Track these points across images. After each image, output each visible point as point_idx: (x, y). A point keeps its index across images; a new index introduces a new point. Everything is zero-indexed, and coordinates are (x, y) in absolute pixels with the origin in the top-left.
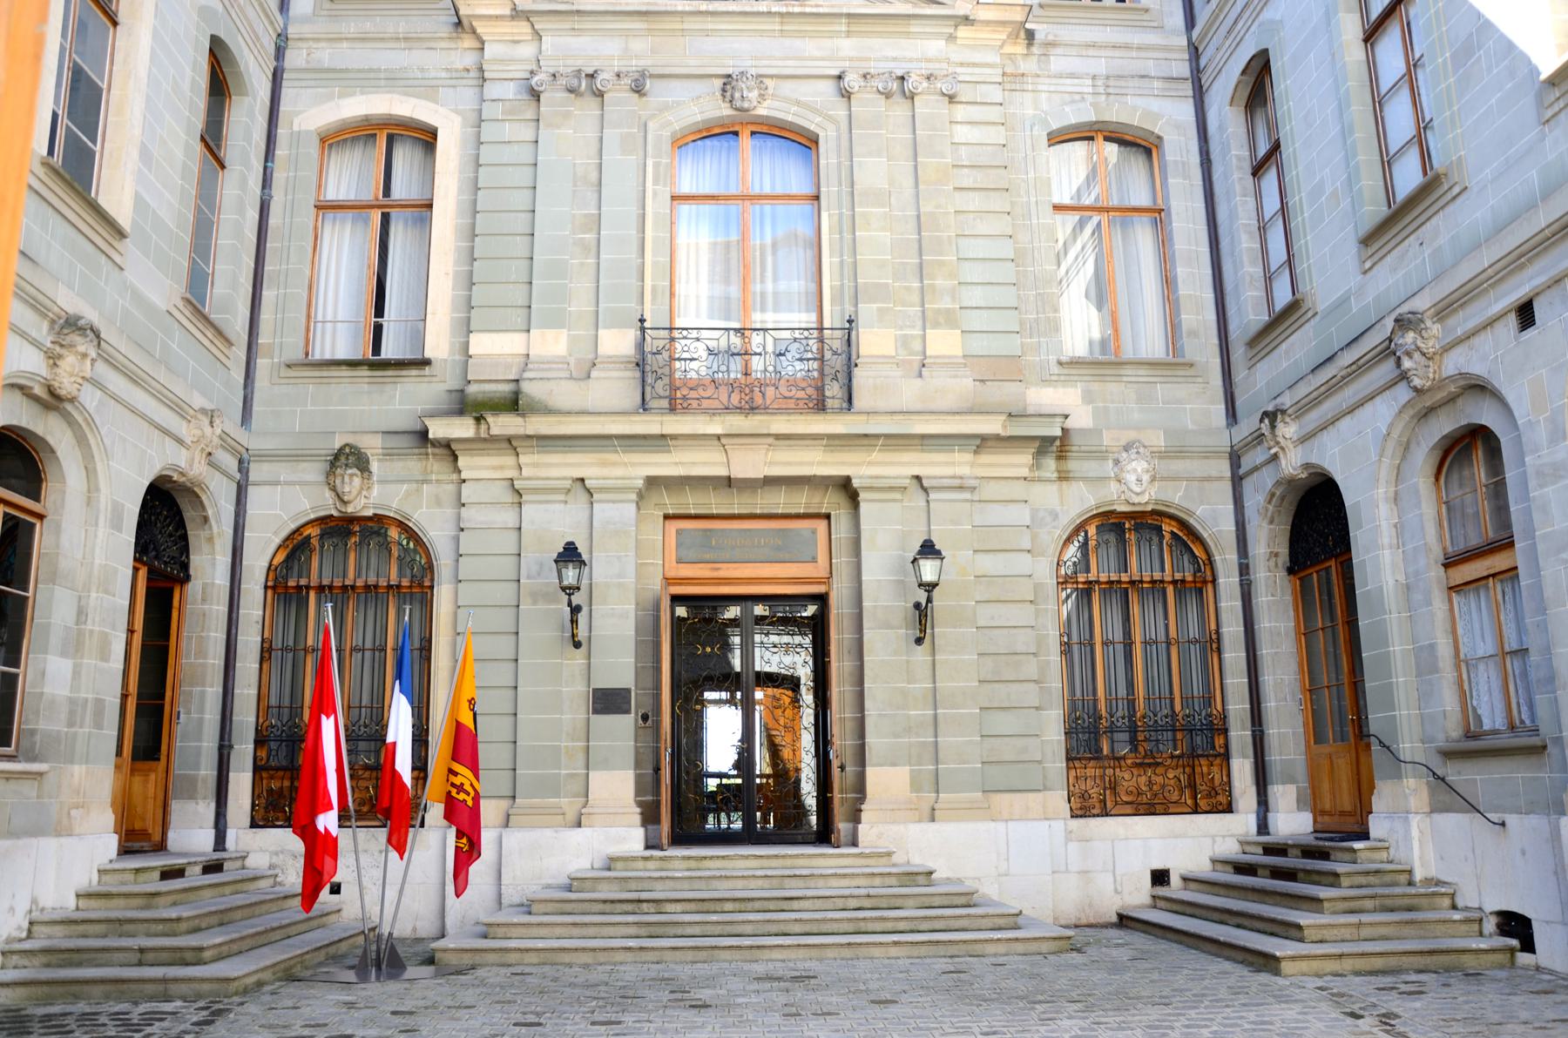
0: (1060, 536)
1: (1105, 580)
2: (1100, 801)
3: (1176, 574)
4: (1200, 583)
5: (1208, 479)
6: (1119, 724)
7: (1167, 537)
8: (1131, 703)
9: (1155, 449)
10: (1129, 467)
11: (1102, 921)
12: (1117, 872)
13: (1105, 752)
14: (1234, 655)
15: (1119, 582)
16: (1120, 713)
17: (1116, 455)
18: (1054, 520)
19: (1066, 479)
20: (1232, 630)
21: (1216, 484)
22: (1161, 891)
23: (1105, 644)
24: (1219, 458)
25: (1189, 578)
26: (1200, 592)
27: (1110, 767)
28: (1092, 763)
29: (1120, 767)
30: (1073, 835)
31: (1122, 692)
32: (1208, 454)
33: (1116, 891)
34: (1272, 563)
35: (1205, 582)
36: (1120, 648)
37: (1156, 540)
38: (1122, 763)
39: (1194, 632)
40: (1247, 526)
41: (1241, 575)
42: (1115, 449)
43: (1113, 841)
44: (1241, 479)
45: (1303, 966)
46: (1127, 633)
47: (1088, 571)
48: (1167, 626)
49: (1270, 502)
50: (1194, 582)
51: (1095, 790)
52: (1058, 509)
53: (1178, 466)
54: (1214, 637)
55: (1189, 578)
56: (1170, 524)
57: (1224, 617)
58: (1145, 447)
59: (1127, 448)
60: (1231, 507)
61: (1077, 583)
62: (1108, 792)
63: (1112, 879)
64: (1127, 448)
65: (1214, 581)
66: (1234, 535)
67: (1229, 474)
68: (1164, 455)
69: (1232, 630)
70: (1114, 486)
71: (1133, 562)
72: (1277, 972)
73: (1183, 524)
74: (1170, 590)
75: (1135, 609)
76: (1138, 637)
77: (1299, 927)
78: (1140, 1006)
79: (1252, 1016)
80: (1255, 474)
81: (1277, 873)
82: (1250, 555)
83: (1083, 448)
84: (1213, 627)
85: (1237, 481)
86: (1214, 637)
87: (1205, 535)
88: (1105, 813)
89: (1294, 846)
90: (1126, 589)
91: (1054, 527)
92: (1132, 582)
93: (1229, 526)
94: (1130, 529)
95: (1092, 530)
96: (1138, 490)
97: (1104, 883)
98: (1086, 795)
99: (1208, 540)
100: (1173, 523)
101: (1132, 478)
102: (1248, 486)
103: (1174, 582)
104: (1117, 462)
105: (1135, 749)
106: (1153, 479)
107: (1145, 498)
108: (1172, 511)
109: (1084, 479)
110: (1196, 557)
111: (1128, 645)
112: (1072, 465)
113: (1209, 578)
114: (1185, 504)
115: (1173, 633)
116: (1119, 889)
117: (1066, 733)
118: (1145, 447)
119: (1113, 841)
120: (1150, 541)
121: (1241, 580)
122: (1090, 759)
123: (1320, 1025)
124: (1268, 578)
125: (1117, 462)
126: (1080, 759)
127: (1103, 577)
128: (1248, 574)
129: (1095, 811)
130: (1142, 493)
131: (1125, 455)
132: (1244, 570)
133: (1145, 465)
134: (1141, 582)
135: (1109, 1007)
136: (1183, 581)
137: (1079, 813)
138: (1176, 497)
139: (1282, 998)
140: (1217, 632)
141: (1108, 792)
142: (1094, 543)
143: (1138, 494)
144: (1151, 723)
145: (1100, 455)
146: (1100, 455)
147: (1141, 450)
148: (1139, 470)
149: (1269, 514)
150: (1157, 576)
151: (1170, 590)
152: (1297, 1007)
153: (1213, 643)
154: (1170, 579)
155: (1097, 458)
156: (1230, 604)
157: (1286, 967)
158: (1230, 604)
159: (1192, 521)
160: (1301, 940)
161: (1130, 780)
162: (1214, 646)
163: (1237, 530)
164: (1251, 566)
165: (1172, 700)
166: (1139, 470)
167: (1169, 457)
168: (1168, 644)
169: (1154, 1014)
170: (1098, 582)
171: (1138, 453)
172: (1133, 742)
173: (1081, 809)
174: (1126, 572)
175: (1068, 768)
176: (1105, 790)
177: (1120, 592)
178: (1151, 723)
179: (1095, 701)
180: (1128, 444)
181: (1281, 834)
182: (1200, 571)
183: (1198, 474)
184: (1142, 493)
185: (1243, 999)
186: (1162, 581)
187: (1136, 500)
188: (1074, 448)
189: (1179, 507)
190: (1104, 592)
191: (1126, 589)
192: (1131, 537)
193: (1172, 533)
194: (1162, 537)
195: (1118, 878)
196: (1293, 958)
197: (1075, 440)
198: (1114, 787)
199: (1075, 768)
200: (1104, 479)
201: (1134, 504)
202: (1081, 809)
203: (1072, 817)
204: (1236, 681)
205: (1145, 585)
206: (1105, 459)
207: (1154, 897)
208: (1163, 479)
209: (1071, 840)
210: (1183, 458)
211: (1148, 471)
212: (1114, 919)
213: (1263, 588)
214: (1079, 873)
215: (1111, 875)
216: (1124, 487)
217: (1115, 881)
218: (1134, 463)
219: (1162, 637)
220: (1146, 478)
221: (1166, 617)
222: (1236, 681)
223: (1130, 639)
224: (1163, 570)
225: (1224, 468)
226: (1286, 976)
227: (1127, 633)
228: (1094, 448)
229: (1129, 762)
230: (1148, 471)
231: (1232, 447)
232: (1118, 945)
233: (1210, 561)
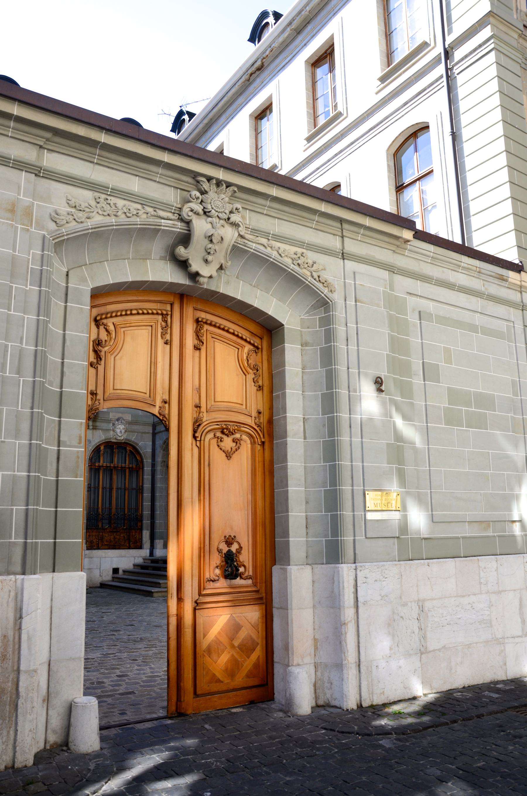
0: (91, 449)
1: (105, 465)
2: (97, 544)
3: (130, 465)
4: (139, 468)
5: (145, 433)
6: (106, 517)
7: (128, 452)
8: (110, 509)
9: (127, 421)
10: (118, 427)
11: (94, 586)
12: (101, 569)
13: (100, 527)
14: (147, 495)
15: (110, 467)
16: (106, 513)
17: (114, 422)
18: (90, 443)
19: (95, 429)
20: (147, 485)
21: (147, 435)
22: (116, 576)
23: (103, 488)
24: (149, 426)
25: (134, 467)
26: (137, 472)
27: (101, 532)
28: (95, 531)
29: (105, 532)
30: (87, 556)
31: (108, 506)
32: (145, 424)
33: (100, 575)
34: (163, 464)
35: (140, 468)
36: (108, 490)
37: (124, 451)
38: (106, 531)
39: (134, 486)
40: (156, 451)
41: (152, 467)
42: (113, 420)
43: (100, 558)
44: (156, 434)
45: (160, 594)
46: (111, 484)
47: (99, 462)
48: (125, 483)
49: (164, 444)
50: (136, 468)
51: (96, 540)
52: (91, 439)
53: (135, 427)
54: (141, 488)
55: (134, 467)
56: (130, 447)
57: (145, 481)
58: (124, 420)
59: (118, 420)
60: (151, 443)
61: (95, 466)
62: (100, 541)
63: (99, 572)
64: (118, 420)
65: (143, 468)
66: (151, 453)
67: (151, 432)
68: (130, 423)
69: (147, 485)
70: (112, 433)
71: (116, 460)
72: (152, 596)
73: (134, 448)
74: (127, 470)
75: (115, 477)
76: (115, 487)
77: (160, 584)
79: (144, 606)
80: (160, 434)
81: (155, 569)
82: (156, 460)
83: (102, 418)
84: (141, 484)
85: (154, 434)
86: (141, 488)
87: (141, 452)
88: (98, 548)
89: (161, 560)
90: (112, 469)
91: (89, 446)
92: (114, 467)
93: (149, 450)
94: (115, 448)
95: (102, 448)
96: (120, 435)
97: (97, 573)
98: (92, 542)
99: (142, 454)
100: (131, 447)
101: (118, 431)
102: (158, 437)
103: (129, 468)
104: (114, 424)
105: (110, 526)
106: (126, 431)
107: (122, 438)
108: (131, 443)
109: (102, 429)
110: (137, 460)
111: (111, 489)
112: (98, 424)
113: (141, 467)
114: (136, 441)
115: (127, 486)
116: (101, 575)
117: (87, 520)
118: (124, 420)
119: (100, 558)
120: (122, 453)
121: (152, 469)
122: (95, 529)
123: (162, 607)
124: (161, 469)
125: (114, 424)
126: (91, 529)
127: (105, 465)
128: (154, 467)
129: (95, 548)
130: (122, 436)
131: (117, 422)
132: (153, 465)
133: (123, 427)
134: (118, 467)
136: (132, 468)
137: (89, 548)
138: (133, 438)
139: (152, 602)
140: (142, 486)
141: (100, 541)
142: (102, 452)
143: (120, 436)
144: (116, 517)
145: (108, 421)
146: (108, 421)
147: (123, 421)
148: (121, 428)
149: (164, 448)
150: (123, 465)
151: (127, 470)
152: (157, 604)
153: (140, 490)
154: (127, 466)
155: (107, 422)
156: (147, 477)
157: (155, 595)
158: (147, 477)
159: (137, 447)
160: (160, 588)
161: (107, 537)
162: (141, 491)
163: (152, 452)
164: (156, 464)
165: (124, 509)
166: (121, 428)
167: (133, 424)
168: (125, 489)
169: (117, 606)
170: (103, 466)
171: (121, 422)
172: (110, 523)
173: (90, 546)
174: (113, 463)
175: (87, 532)
176: (99, 540)
177: (110, 470)
178: (116, 517)
179: (98, 509)
180: (118, 418)
181: (157, 556)
182: (138, 464)
183: (141, 431)
184: (122, 436)
185: (142, 603)
186: (125, 467)
187: (119, 438)
188: (99, 418)
189: (133, 442)
190: (104, 470)
191: (112, 469)
192: (116, 451)
193: (130, 450)
194: (126, 452)
195: (101, 571)
196: (157, 592)
197: (100, 415)
198: (102, 539)
199: (89, 532)
200: (109, 430)
201: (118, 440)
202: (90, 546)
203: (87, 549)
204: (147, 504)
205: (119, 468)
206: (110, 423)
207: (113, 578)
208: (129, 432)
209: (86, 558)
210: (137, 425)
211: (124, 429)
212: (99, 585)
213: (159, 473)
214: (88, 569)
215: (99, 570)
216: (115, 434)
217: (100, 572)
218: (120, 426)
219: (123, 487)
220: (123, 431)
221: (125, 480)
222: (147, 504)
223: (112, 487)
224: (125, 463)
225: (150, 429)
226: (154, 597)
227: (111, 484)
228: (106, 419)
229: (108, 530)
230: (124, 429)
231: (154, 422)
232: (102, 592)
233: (142, 461)
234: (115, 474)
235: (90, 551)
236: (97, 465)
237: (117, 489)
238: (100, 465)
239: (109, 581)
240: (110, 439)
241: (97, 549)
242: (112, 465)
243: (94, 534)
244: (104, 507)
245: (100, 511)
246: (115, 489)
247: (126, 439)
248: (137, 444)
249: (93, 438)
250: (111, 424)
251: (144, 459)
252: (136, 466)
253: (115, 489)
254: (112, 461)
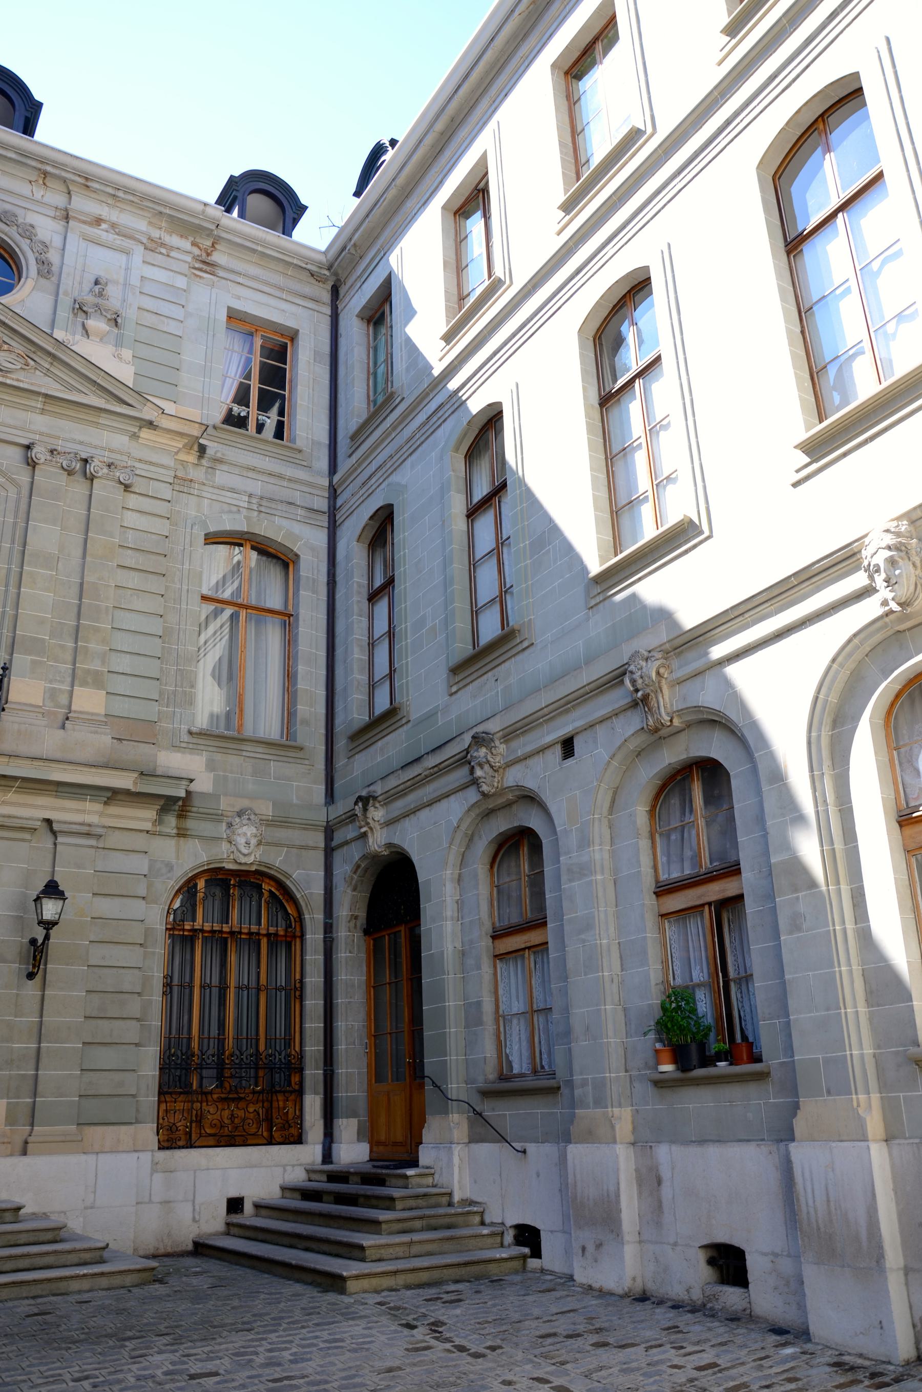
0: (173, 886)
2: (186, 1133)
3: (270, 928)
6: (209, 1061)
7: (266, 894)
8: (221, 1042)
9: (264, 817)
10: (240, 831)
12: (197, 1202)
13: (194, 1088)
14: (314, 1003)
15: (221, 932)
16: (211, 1052)
18: (169, 871)
20: (314, 979)
22: (236, 1219)
23: (202, 987)
24: (315, 830)
25: (281, 933)
26: (289, 946)
27: (198, 1101)
28: (182, 1098)
29: (207, 1101)
31: (214, 1032)
32: (308, 826)
33: (194, 1220)
34: (352, 924)
35: (294, 937)
36: (215, 991)
37: (256, 897)
38: (209, 1097)
41: (325, 933)
42: (229, 814)
43: (195, 1171)
44: (333, 850)
45: (365, 1283)
47: (194, 920)
48: (258, 974)
49: (355, 873)
50: (285, 936)
52: (174, 861)
53: (281, 834)
54: (298, 985)
55: (281, 933)
56: (268, 884)
57: (308, 968)
58: (256, 815)
60: (322, 873)
61: (184, 930)
62: (194, 1125)
63: (191, 1209)
64: (240, 814)
65: (302, 936)
67: (322, 845)
68: (271, 823)
69: (314, 979)
70: (225, 846)
71: (235, 914)
72: (342, 1291)
75: (232, 958)
76: (233, 983)
77: (362, 1248)
78: (225, 1333)
79: (325, 1335)
80: (345, 847)
81: (341, 1199)
83: (201, 810)
84: (298, 977)
85: (329, 851)
86: (298, 985)
87: (298, 896)
88: (190, 1145)
89: (355, 1174)
90: (226, 939)
91: (168, 878)
92: (232, 933)
93: (318, 889)
94: (234, 886)
95: (201, 884)
96: (245, 851)
97: (184, 1212)
98: (174, 1128)
99: (301, 901)
100: (272, 883)
101: (241, 841)
102: (338, 856)
103: (268, 935)
104: (230, 825)
105: (220, 1085)
106: (259, 843)
107: (251, 859)
108: (272, 872)
109: (199, 837)
111: (223, 988)
112: (191, 824)
113: (298, 933)
116: (197, 1217)
117: (160, 1069)
118: (256, 815)
119: (195, 1171)
121: (325, 938)
122: (181, 1093)
123: (383, 1338)
124: (347, 937)
125: (230, 825)
126: (171, 1093)
127: (207, 927)
128: (331, 932)
129: (181, 1143)
131: (237, 820)
132: (328, 928)
133: (254, 831)
134: (240, 933)
135: (195, 1337)
136: (276, 935)
137: (165, 1144)
138: (277, 860)
139: (349, 1315)
140: (301, 981)
141: (194, 1125)
142: (202, 895)
143: (245, 855)
144: (237, 1061)
145: (217, 817)
146: (217, 817)
147: (252, 817)
148: (249, 834)
149: (354, 882)
150: (254, 928)
152: (363, 1323)
153: (296, 991)
154: (264, 932)
156: (314, 958)
157: (351, 1286)
158: (314, 958)
159: (288, 883)
160: (363, 1260)
161: (213, 1113)
162: (298, 993)
163: (325, 894)
164: (334, 926)
165: (257, 1040)
166: (249, 834)
168: (258, 989)
169: (238, 1341)
170: (202, 931)
171: (249, 819)
172: (220, 1078)
173: (168, 1141)
174: (227, 923)
175: (159, 1102)
179: (190, 1039)
181: (342, 1162)
182: (290, 926)
183: (297, 843)
185: (316, 1319)
186: (258, 934)
187: (243, 860)
188: (194, 809)
189: (279, 870)
191: (226, 939)
192: (235, 892)
193: (270, 891)
194: (261, 895)
195: (197, 1207)
196: (357, 1277)
197: (196, 802)
199: (166, 1102)
201: (240, 864)
202: (168, 1141)
203: (159, 1149)
204: (314, 1025)
205: (243, 936)
206: (220, 821)
207: (228, 1224)
208: (268, 844)
209: (157, 1172)
210: (287, 827)
211: (255, 836)
212: (190, 1247)
214: (161, 1203)
216: (233, 848)
217: (194, 1210)
219: (253, 984)
220: (254, 842)
221: (259, 966)
222: (314, 1025)
224: (259, 924)
225: (319, 839)
226: (350, 1295)
228: (211, 811)
229: (215, 1096)
231: (328, 822)
232: (196, 1274)
234: (234, 949)
235: (168, 1153)
236: (187, 927)
237: (239, 988)
238: (196, 927)
239: (217, 1234)
240: (221, 861)
241: (187, 1148)
242: (226, 928)
243: (179, 1106)
244: (206, 1035)
245: (195, 1044)
246: (232, 989)
247: (260, 863)
248: (289, 876)
249: (178, 858)
250: (224, 824)
251: (305, 912)
252: (286, 931)
253: (232, 989)
254: (225, 919)
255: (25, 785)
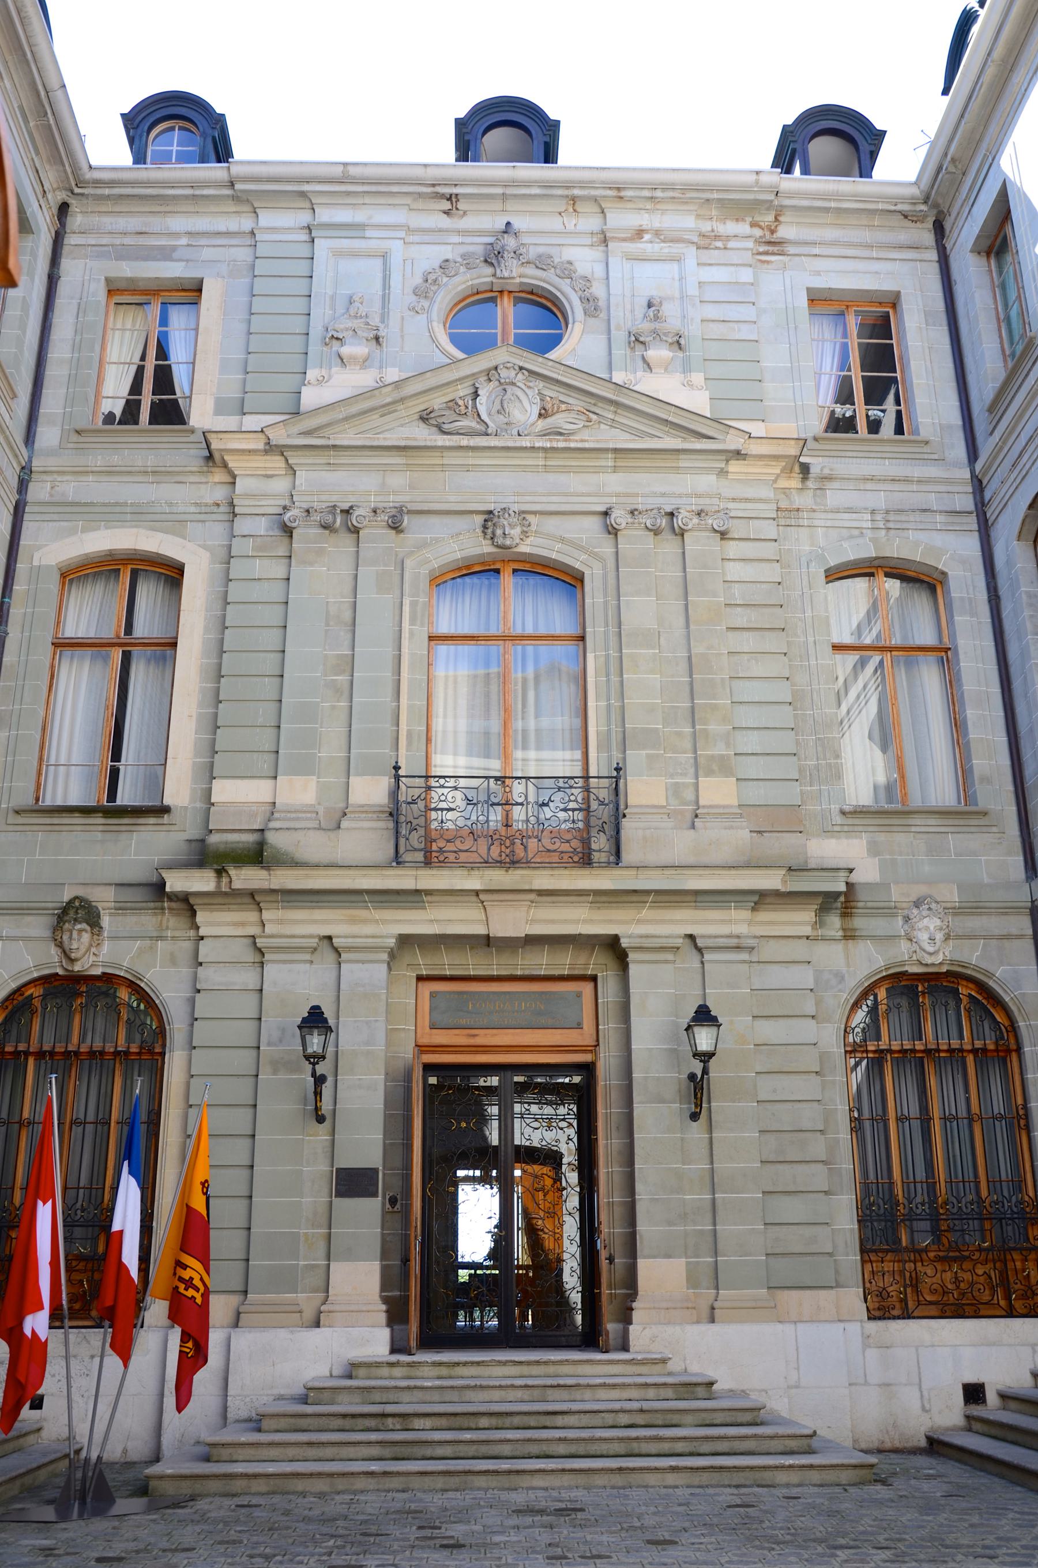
2: (901, 1301)
3: (976, 1042)
5: (1008, 937)
6: (919, 1211)
7: (965, 1000)
8: (931, 1187)
9: (949, 905)
10: (920, 925)
11: (909, 1445)
12: (924, 1387)
13: (904, 1244)
15: (914, 1051)
16: (919, 1199)
17: (906, 912)
19: (852, 937)
21: (1017, 943)
22: (976, 1410)
23: (900, 1119)
24: (1018, 914)
25: (991, 1047)
26: (1004, 1062)
27: (910, 1261)
28: (890, 1256)
29: (922, 1261)
30: (871, 1340)
31: (921, 1174)
32: (1007, 910)
33: (924, 1409)
35: (1008, 1051)
36: (916, 1124)
37: (952, 1004)
38: (924, 1256)
39: (999, 1107)
42: (904, 905)
43: (917, 1348)
47: (878, 1038)
48: (968, 1100)
50: (997, 1050)
52: (844, 970)
55: (991, 1047)
58: (937, 902)
59: (917, 904)
61: (867, 1052)
62: (909, 1290)
64: (917, 904)
65: (1019, 1050)
68: (958, 911)
70: (904, 946)
73: (982, 987)
74: (970, 1059)
75: (932, 1082)
76: (936, 1113)
78: (959, 1557)
83: (869, 904)
84: (1020, 1101)
86: (1021, 1112)
87: (1007, 999)
88: (906, 1315)
91: (840, 991)
92: (928, 1052)
94: (923, 993)
95: (882, 994)
96: (931, 949)
97: (910, 1399)
99: (1011, 1004)
101: (923, 937)
103: (974, 1051)
104: (907, 919)
105: (937, 1240)
106: (947, 938)
108: (969, 972)
111: (926, 1120)
112: (858, 922)
113: (1013, 1046)
114: (983, 965)
115: (975, 1109)
116: (927, 1407)
117: (859, 1221)
118: (937, 902)
122: (887, 1251)
125: (907, 919)
126: (875, 1251)
127: (896, 1046)
129: (896, 1312)
131: (915, 911)
133: (938, 922)
134: (938, 1050)
135: (922, 1556)
136: (984, 1050)
137: (877, 1314)
140: (1025, 1106)
141: (909, 1290)
142: (884, 1007)
143: (931, 954)
144: (955, 1210)
145: (889, 911)
146: (889, 911)
147: (933, 906)
148: (932, 928)
150: (955, 1043)
151: (970, 1059)
154: (969, 1047)
159: (991, 983)
161: (931, 1275)
162: (1022, 1122)
165: (977, 1183)
166: (932, 928)
168: (971, 1119)
170: (890, 1051)
171: (930, 909)
172: (936, 1233)
173: (879, 1309)
174: (921, 1039)
175: (863, 1262)
178: (955, 1210)
179: (891, 1184)
182: (1002, 1038)
183: (997, 932)
186: (961, 1050)
187: (929, 960)
188: (860, 904)
189: (977, 968)
190: (896, 1062)
192: (926, 1001)
193: (970, 996)
195: (925, 1393)
197: (862, 895)
198: (915, 1284)
199: (871, 1261)
201: (927, 965)
202: (879, 1309)
203: (869, 1318)
205: (942, 1055)
206: (894, 915)
207: (968, 1417)
208: (959, 937)
209: (870, 1347)
210: (980, 914)
211: (941, 929)
212: (923, 1443)
214: (879, 1385)
216: (915, 947)
217: (922, 1396)
218: (926, 920)
219: (963, 1112)
220: (939, 936)
221: (967, 1090)
223: (927, 1113)
229: (932, 1255)
230: (941, 929)
231: (1032, 902)
232: (929, 1477)
234: (932, 1071)
235: (881, 1324)
236: (871, 1048)
237: (944, 1119)
238: (881, 1047)
239: (954, 1429)
240: (902, 963)
241: (904, 1318)
242: (919, 1046)
243: (888, 1266)
244: (911, 1179)
245: (899, 1190)
246: (937, 1121)
247: (952, 962)
248: (990, 975)
249: (848, 965)
250: (900, 918)
251: (1019, 1018)
252: (996, 1044)
253: (937, 1121)
254: (918, 1034)
255: (598, 899)
